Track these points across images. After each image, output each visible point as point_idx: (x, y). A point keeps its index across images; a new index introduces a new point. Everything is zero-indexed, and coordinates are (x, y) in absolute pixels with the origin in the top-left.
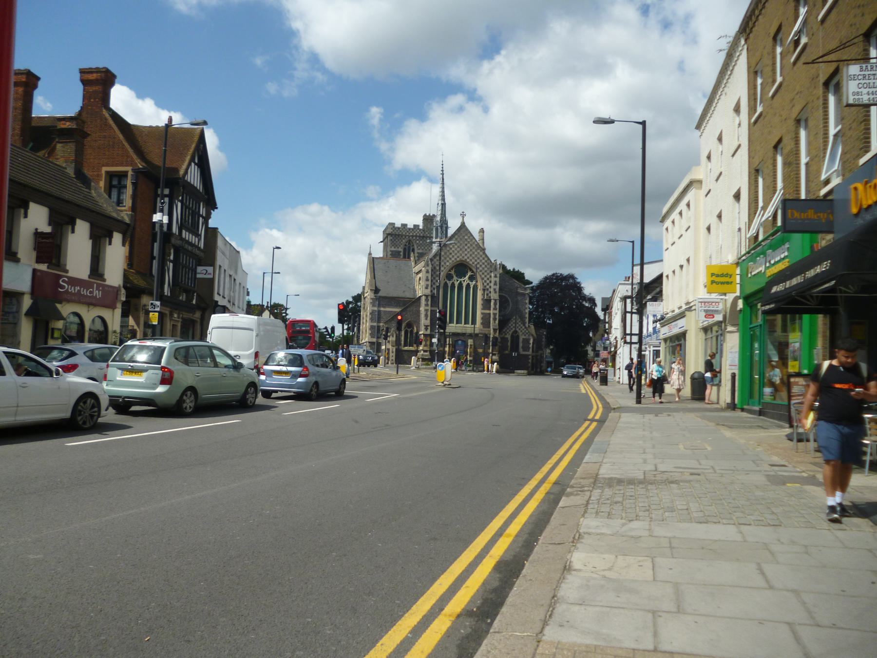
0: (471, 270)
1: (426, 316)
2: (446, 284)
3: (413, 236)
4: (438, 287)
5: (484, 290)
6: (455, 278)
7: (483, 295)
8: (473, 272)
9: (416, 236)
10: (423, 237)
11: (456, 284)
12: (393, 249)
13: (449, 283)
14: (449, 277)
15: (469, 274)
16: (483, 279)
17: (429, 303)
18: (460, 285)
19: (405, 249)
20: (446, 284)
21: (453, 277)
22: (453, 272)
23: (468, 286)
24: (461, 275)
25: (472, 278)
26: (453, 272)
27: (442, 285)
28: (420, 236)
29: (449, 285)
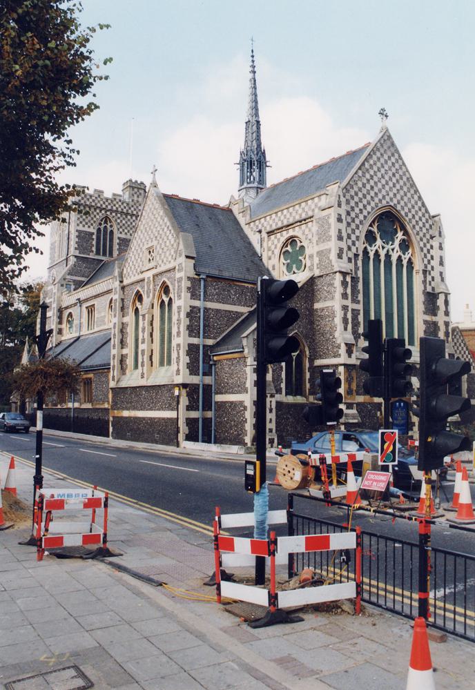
0: (403, 228)
1: (345, 321)
2: (366, 252)
3: (111, 211)
4: (356, 256)
5: (425, 272)
6: (379, 242)
7: (424, 282)
8: (406, 233)
9: (117, 211)
10: (127, 214)
11: (382, 253)
12: (81, 228)
14: (370, 237)
15: (400, 235)
16: (422, 250)
17: (349, 291)
18: (388, 256)
19: (99, 230)
20: (366, 252)
21: (375, 240)
22: (375, 229)
23: (400, 259)
24: (388, 236)
25: (405, 245)
26: (375, 229)
27: (361, 253)
28: (122, 213)
29: (371, 255)
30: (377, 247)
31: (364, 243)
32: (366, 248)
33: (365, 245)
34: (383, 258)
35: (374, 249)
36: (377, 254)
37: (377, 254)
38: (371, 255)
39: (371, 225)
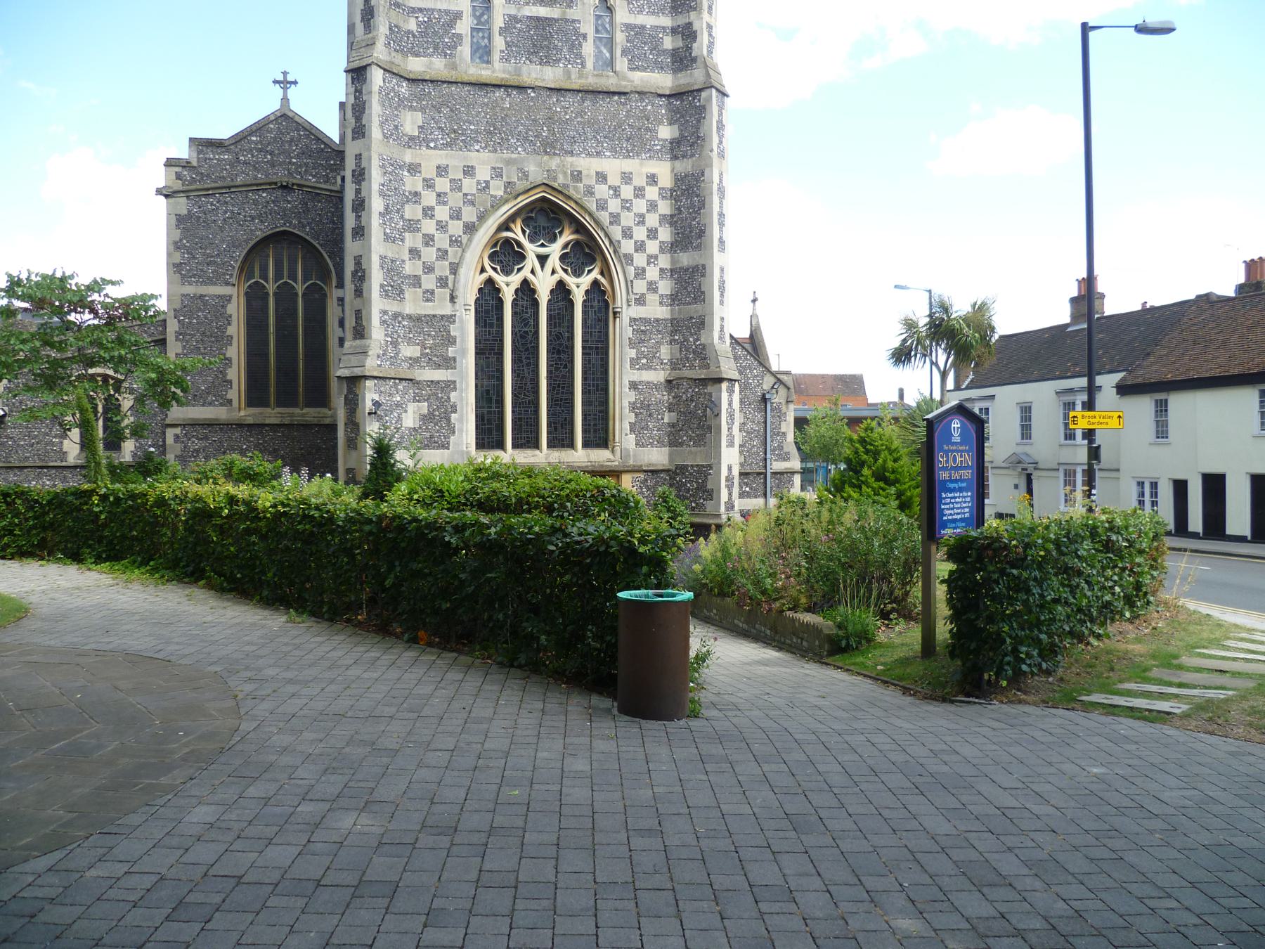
2: (490, 291)
13: (508, 286)
14: (506, 254)
21: (522, 257)
22: (517, 233)
26: (517, 233)
29: (508, 296)
30: (526, 273)
31: (483, 270)
32: (490, 281)
33: (485, 276)
34: (544, 297)
35: (516, 279)
36: (526, 290)
37: (526, 290)
38: (508, 296)
39: (505, 226)
